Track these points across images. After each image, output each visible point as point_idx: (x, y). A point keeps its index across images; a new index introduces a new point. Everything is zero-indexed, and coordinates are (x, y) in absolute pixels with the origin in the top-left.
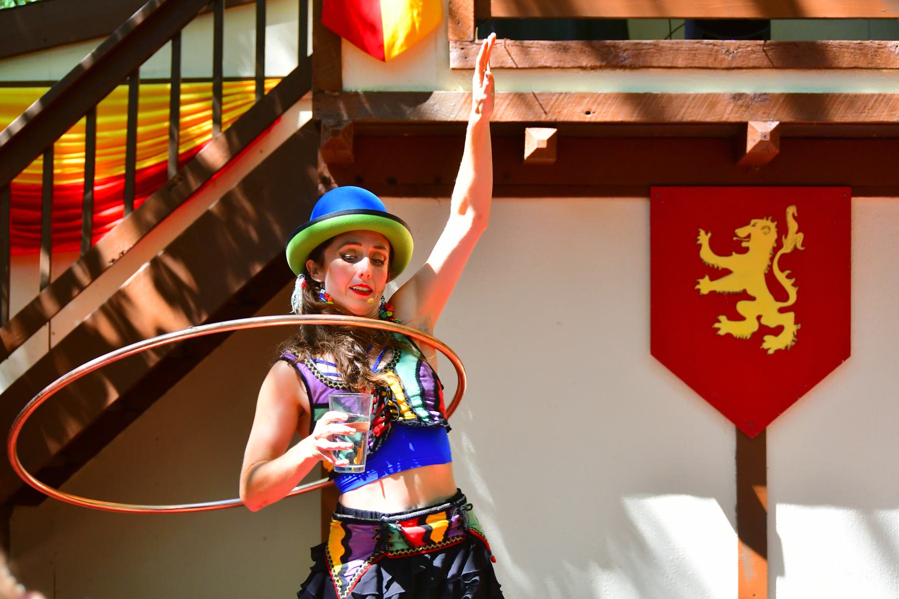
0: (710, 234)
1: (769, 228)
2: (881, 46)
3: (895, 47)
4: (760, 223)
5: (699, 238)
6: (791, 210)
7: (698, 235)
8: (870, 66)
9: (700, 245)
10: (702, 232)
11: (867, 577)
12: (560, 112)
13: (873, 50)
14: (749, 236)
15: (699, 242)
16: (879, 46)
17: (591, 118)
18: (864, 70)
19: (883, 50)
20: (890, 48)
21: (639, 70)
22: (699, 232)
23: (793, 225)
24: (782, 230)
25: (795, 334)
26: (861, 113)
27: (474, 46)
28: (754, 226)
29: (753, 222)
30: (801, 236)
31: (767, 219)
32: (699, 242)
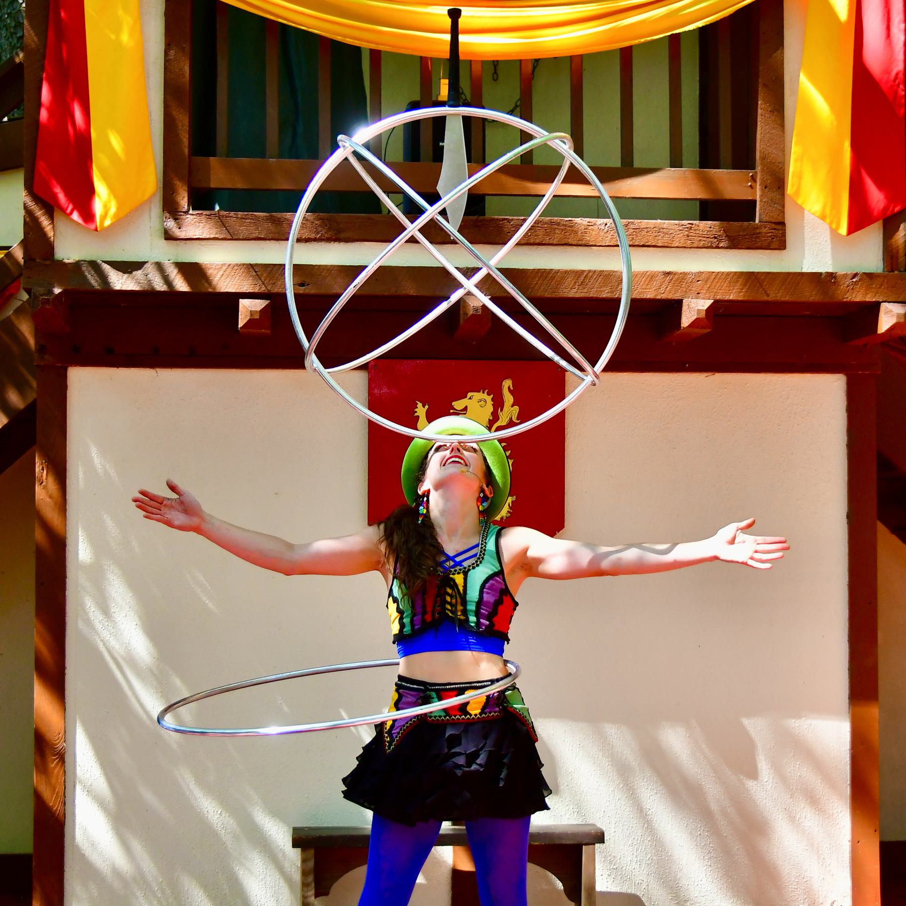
0: (427, 407)
1: (486, 401)
2: (591, 224)
3: (604, 224)
4: (477, 396)
5: (416, 410)
6: (507, 384)
7: (417, 408)
8: (580, 243)
9: (418, 417)
10: (420, 405)
11: (580, 745)
12: (274, 284)
13: (583, 227)
14: (466, 409)
15: (416, 414)
16: (589, 224)
17: (305, 289)
18: (575, 247)
19: (592, 227)
20: (599, 226)
21: (354, 243)
22: (418, 404)
23: (508, 399)
24: (498, 404)
25: (511, 505)
26: (571, 289)
27: (188, 216)
28: (470, 398)
29: (470, 395)
30: (516, 408)
31: (483, 393)
32: (416, 414)
